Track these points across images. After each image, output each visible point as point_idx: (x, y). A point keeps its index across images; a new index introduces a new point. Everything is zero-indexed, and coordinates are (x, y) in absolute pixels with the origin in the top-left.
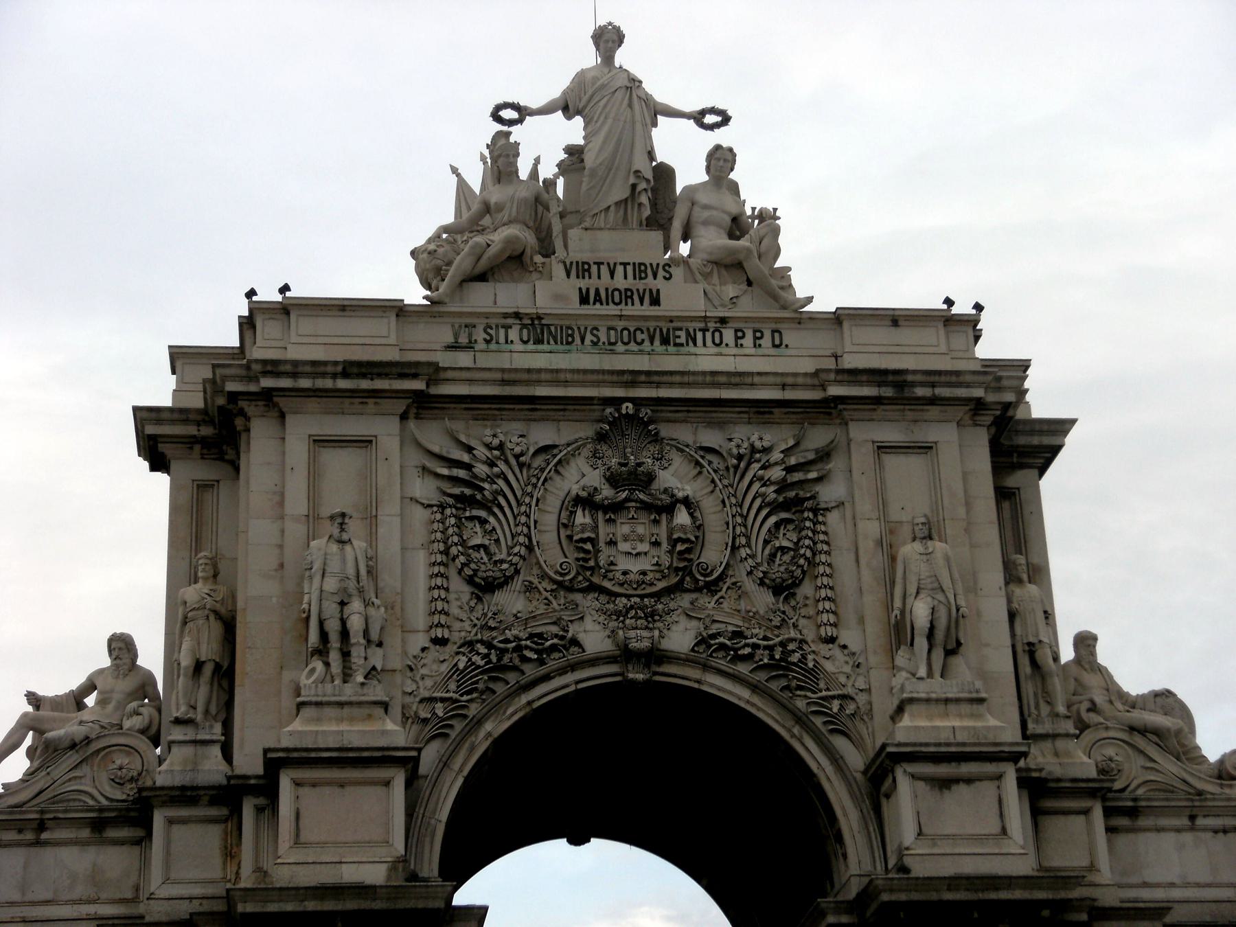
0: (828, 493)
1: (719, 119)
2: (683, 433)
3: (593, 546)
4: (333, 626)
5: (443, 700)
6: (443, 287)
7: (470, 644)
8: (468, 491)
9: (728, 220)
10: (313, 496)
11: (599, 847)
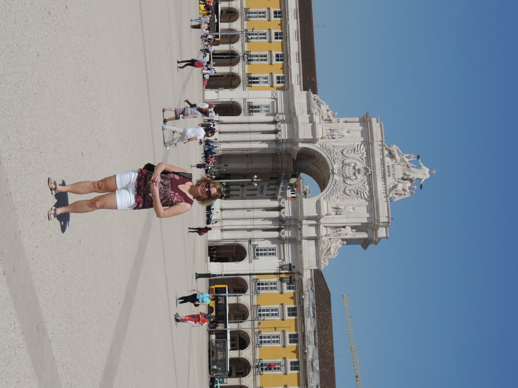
0: (359, 199)
3: (349, 166)
5: (326, 147)
7: (334, 150)
8: (356, 150)
10: (353, 130)
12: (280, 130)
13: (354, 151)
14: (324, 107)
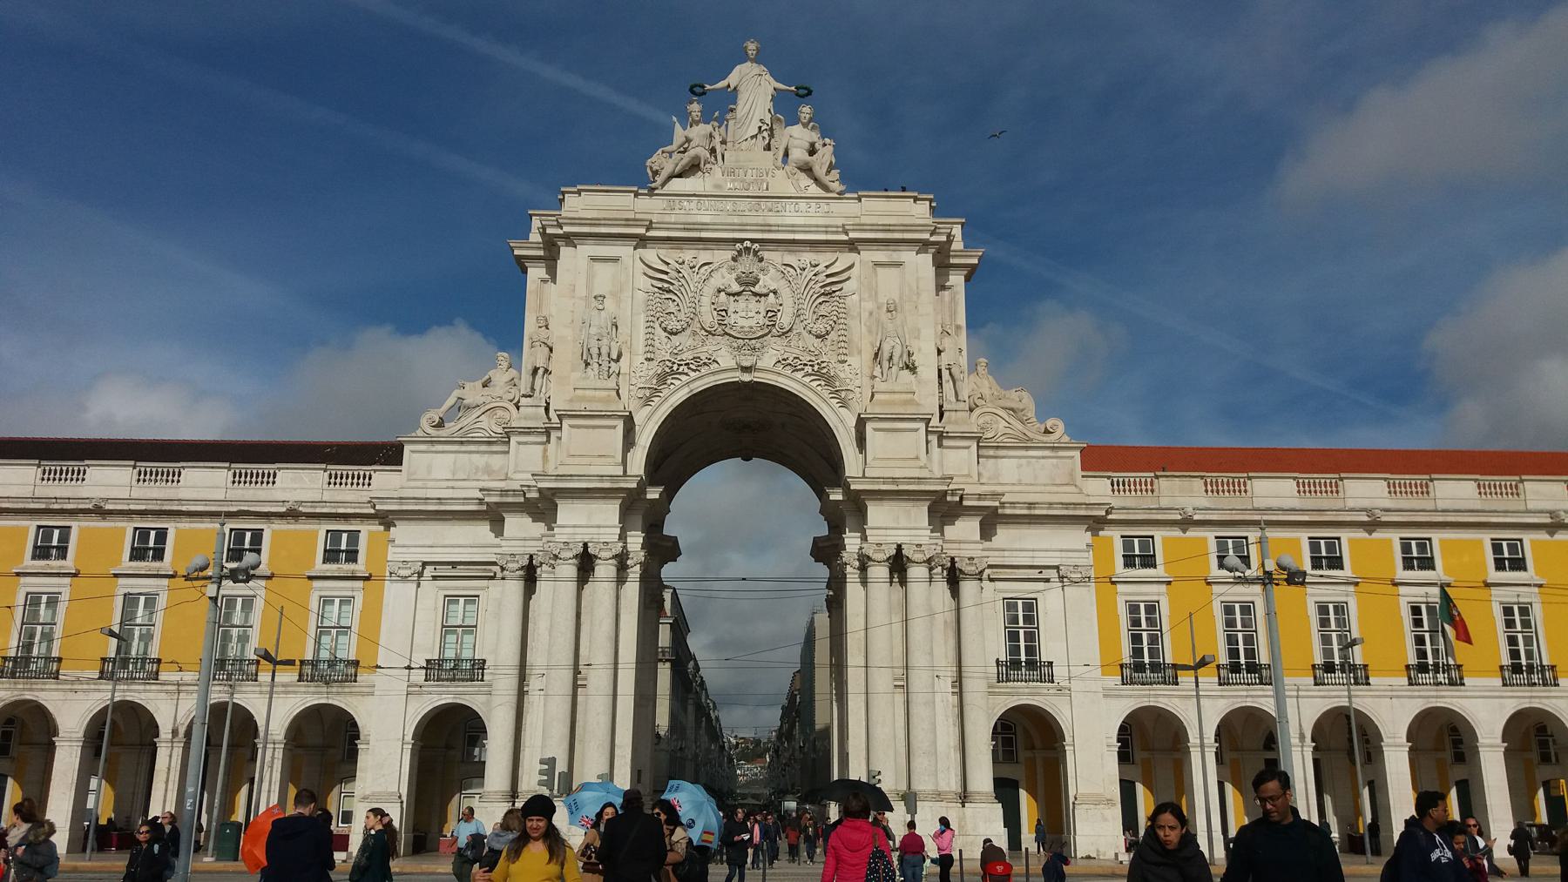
1: (806, 92)
2: (773, 257)
4: (594, 351)
6: (659, 180)
8: (666, 285)
9: (807, 145)
10: (589, 286)
11: (756, 461)
12: (581, 545)
13: (669, 291)
14: (473, 393)
